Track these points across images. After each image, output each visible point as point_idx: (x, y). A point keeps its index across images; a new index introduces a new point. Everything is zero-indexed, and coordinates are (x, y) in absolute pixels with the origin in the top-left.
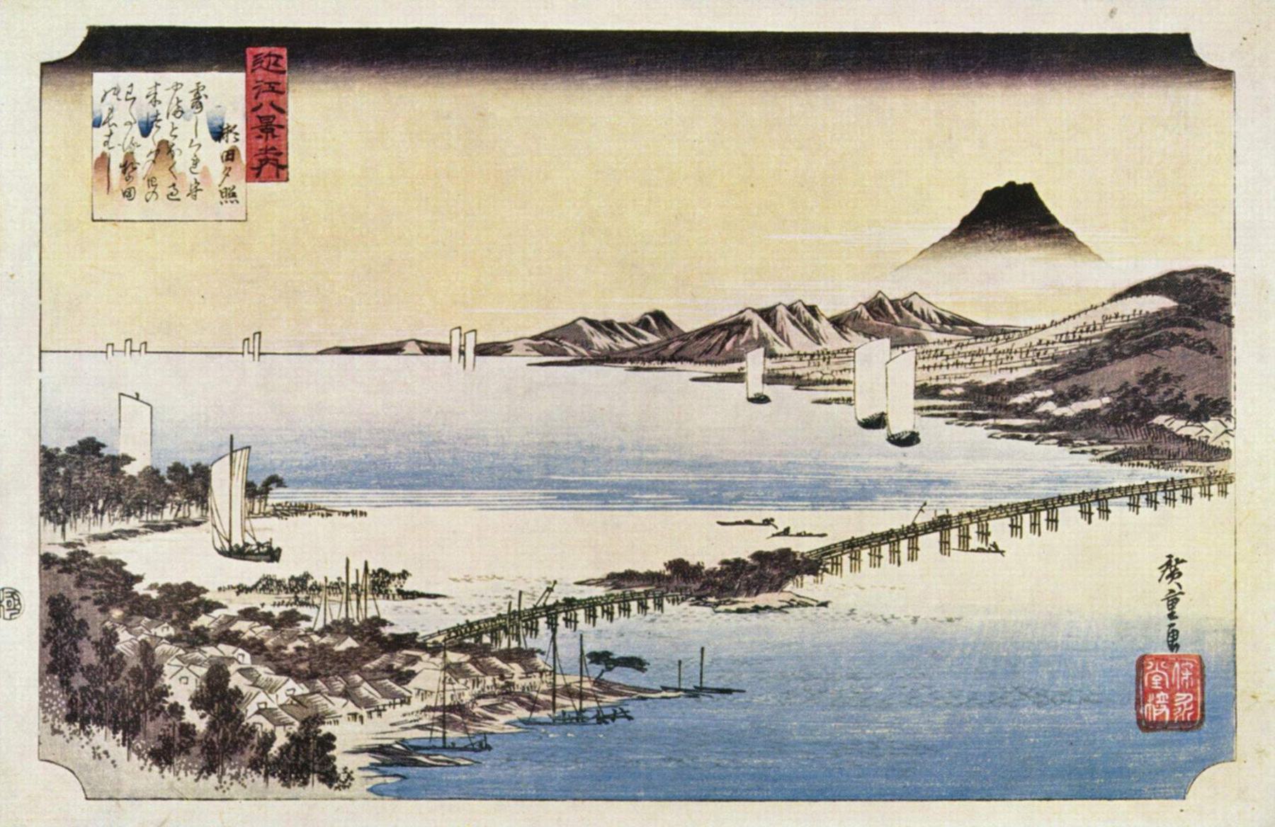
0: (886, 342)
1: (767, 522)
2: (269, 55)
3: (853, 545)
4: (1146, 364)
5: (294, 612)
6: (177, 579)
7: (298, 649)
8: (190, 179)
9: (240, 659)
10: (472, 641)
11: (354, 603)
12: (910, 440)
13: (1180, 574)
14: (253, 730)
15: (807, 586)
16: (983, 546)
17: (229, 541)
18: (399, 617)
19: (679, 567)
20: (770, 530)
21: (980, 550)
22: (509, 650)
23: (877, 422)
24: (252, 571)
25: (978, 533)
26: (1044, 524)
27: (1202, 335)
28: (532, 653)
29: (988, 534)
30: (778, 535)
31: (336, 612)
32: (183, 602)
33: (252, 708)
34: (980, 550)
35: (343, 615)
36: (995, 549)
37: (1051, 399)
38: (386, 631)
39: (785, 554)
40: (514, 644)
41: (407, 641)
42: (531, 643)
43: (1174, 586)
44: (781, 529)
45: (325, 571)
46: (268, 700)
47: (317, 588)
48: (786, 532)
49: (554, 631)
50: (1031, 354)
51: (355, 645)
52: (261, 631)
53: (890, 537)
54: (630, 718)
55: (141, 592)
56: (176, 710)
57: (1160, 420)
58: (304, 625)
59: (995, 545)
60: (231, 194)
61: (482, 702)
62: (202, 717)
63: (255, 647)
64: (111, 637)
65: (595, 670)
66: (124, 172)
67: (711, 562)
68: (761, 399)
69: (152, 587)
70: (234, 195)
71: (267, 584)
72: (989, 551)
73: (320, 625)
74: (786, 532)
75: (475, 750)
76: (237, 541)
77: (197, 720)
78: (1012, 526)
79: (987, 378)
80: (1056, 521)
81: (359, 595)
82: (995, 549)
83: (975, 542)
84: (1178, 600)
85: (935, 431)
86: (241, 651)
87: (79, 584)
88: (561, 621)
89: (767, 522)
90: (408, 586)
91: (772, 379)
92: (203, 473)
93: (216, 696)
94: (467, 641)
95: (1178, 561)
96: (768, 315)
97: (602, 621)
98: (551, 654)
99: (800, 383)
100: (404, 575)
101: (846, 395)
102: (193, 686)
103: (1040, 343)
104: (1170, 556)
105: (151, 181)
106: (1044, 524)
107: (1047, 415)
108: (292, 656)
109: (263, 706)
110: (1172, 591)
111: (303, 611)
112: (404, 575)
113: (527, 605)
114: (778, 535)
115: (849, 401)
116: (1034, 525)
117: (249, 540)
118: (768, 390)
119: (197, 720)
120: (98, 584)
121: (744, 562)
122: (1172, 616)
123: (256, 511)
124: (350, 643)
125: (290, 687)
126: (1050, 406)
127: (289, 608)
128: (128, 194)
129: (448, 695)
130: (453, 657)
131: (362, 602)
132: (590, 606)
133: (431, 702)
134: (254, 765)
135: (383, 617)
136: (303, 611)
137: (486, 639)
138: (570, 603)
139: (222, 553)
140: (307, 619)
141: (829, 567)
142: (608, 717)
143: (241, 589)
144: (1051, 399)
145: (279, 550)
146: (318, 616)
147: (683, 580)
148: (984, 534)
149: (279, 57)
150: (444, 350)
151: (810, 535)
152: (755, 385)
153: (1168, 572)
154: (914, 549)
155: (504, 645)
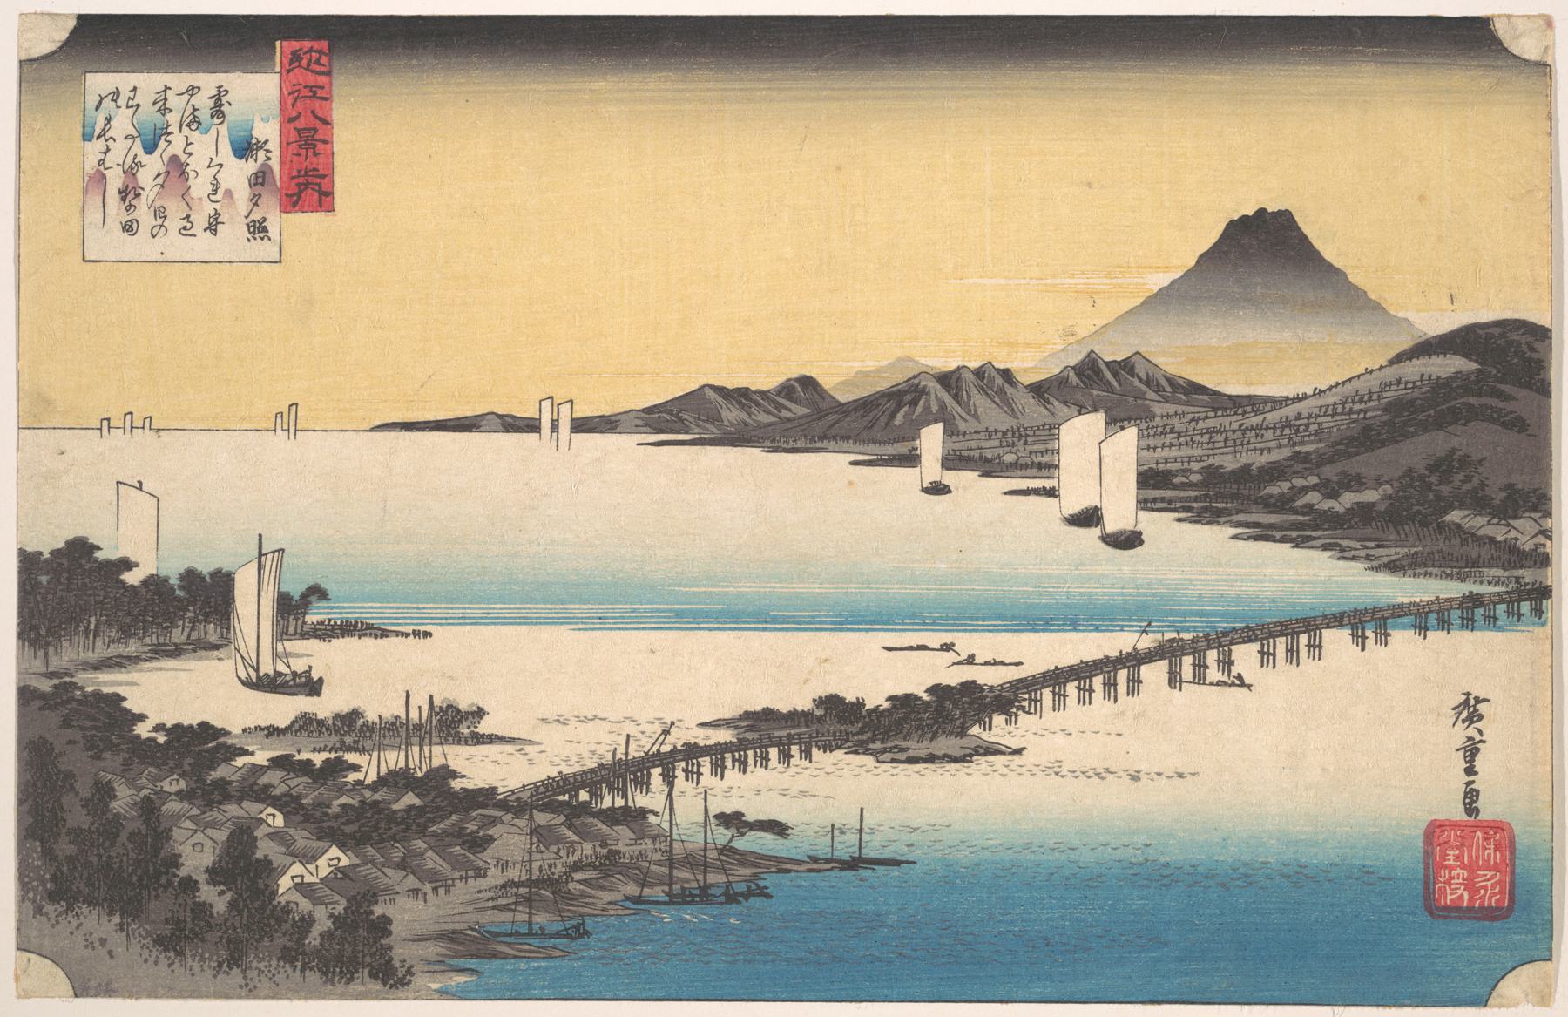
0: (1099, 419)
1: (947, 647)
2: (311, 50)
3: (1057, 678)
4: (1435, 443)
5: (339, 760)
6: (191, 718)
7: (343, 806)
8: (209, 208)
9: (270, 820)
10: (566, 797)
11: (416, 749)
12: (1128, 540)
13: (1481, 717)
14: (287, 910)
15: (999, 730)
16: (1225, 678)
17: (257, 670)
18: (477, 768)
19: (832, 704)
20: (950, 657)
21: (1220, 683)
22: (612, 809)
23: (1088, 518)
24: (282, 709)
25: (1218, 661)
26: (1303, 650)
27: (1509, 406)
28: (643, 813)
29: (1231, 663)
30: (960, 663)
31: (393, 759)
32: (198, 745)
33: (285, 883)
34: (1220, 683)
35: (402, 764)
36: (1241, 682)
37: (1314, 487)
38: (456, 784)
39: (970, 687)
40: (619, 802)
41: (485, 796)
42: (641, 800)
43: (1472, 732)
44: (964, 657)
45: (379, 706)
46: (306, 873)
47: (369, 728)
48: (970, 660)
49: (671, 785)
50: (1287, 431)
51: (417, 801)
52: (298, 783)
53: (1106, 666)
54: (768, 896)
55: (145, 735)
56: (189, 885)
57: (1455, 516)
58: (353, 777)
59: (1239, 677)
60: (258, 229)
61: (578, 876)
62: (221, 893)
63: (288, 804)
64: (105, 792)
65: (722, 835)
66: (124, 200)
67: (876, 698)
68: (938, 489)
69: (159, 728)
70: (265, 230)
71: (305, 724)
72: (1233, 684)
73: (372, 777)
74: (970, 660)
75: (568, 936)
76: (266, 668)
77: (216, 899)
78: (1262, 653)
79: (1229, 463)
80: (1320, 647)
81: (422, 738)
82: (1241, 682)
83: (1214, 674)
84: (1478, 750)
85: (1159, 527)
86: (270, 810)
87: (66, 723)
88: (679, 773)
89: (947, 647)
90: (485, 727)
91: (952, 461)
92: (223, 583)
93: (243, 868)
94: (561, 798)
95: (1478, 700)
96: (949, 380)
97: (732, 775)
98: (667, 817)
99: (989, 468)
100: (480, 713)
101: (1048, 484)
102: (207, 858)
103: (1299, 416)
104: (1468, 694)
105: (160, 213)
106: (1303, 650)
107: (1309, 509)
108: (337, 817)
109: (298, 880)
110: (1470, 739)
111: (351, 758)
112: (480, 713)
113: (635, 752)
114: (960, 663)
115: (1051, 493)
116: (1292, 652)
117: (281, 668)
118: (949, 478)
119: (216, 899)
120: (88, 724)
121: (917, 698)
122: (1470, 771)
123: (291, 630)
124: (410, 799)
125: (334, 857)
126: (1313, 497)
127: (333, 755)
128: (129, 228)
129: (536, 865)
130: (542, 818)
131: (426, 749)
132: (717, 753)
133: (514, 874)
134: (288, 956)
135: (453, 766)
136: (351, 758)
137: (584, 796)
138: (691, 751)
139: (247, 684)
140: (355, 768)
141: (1025, 703)
142: (741, 894)
143: (272, 731)
144: (1314, 487)
145: (321, 680)
146: (368, 766)
147: (840, 724)
148: (1226, 663)
149: (321, 52)
150: (532, 426)
151: (1002, 663)
152: (931, 468)
153: (1465, 715)
154: (1135, 684)
155: (607, 802)
